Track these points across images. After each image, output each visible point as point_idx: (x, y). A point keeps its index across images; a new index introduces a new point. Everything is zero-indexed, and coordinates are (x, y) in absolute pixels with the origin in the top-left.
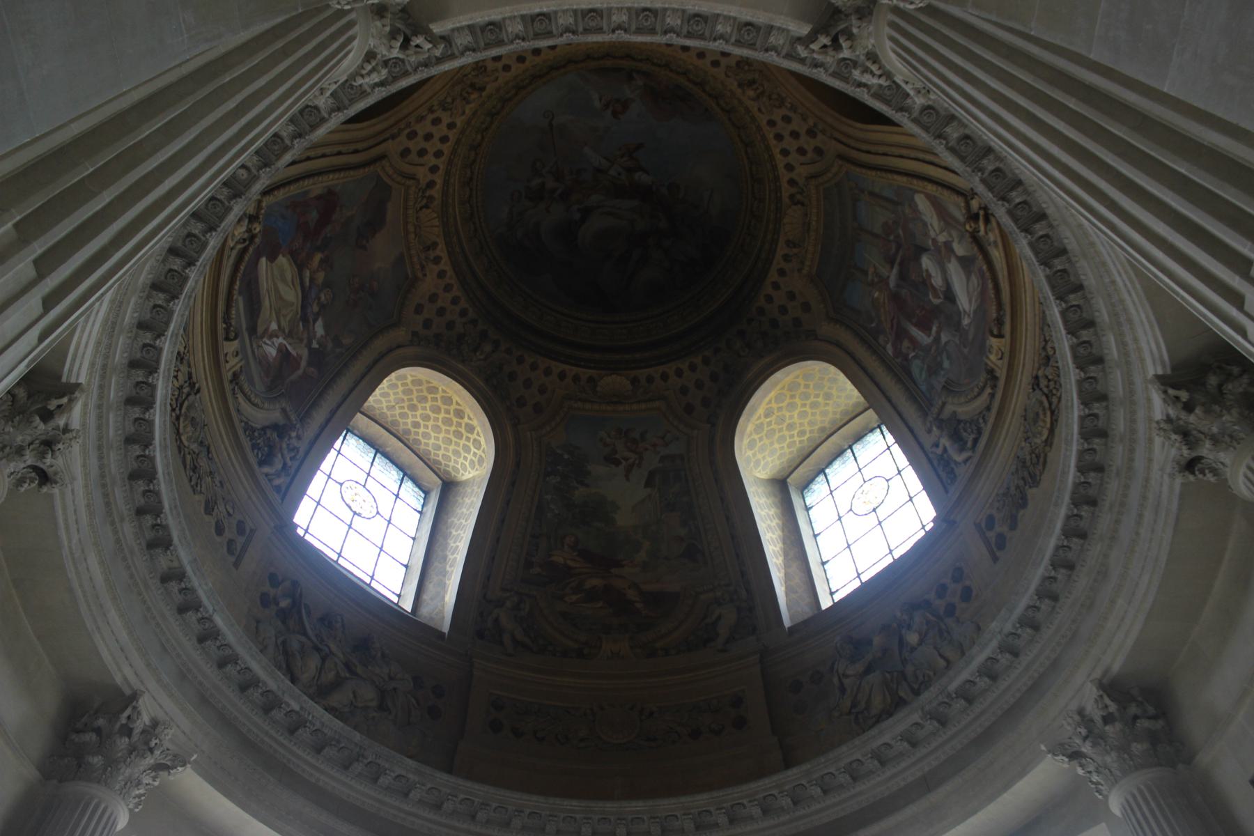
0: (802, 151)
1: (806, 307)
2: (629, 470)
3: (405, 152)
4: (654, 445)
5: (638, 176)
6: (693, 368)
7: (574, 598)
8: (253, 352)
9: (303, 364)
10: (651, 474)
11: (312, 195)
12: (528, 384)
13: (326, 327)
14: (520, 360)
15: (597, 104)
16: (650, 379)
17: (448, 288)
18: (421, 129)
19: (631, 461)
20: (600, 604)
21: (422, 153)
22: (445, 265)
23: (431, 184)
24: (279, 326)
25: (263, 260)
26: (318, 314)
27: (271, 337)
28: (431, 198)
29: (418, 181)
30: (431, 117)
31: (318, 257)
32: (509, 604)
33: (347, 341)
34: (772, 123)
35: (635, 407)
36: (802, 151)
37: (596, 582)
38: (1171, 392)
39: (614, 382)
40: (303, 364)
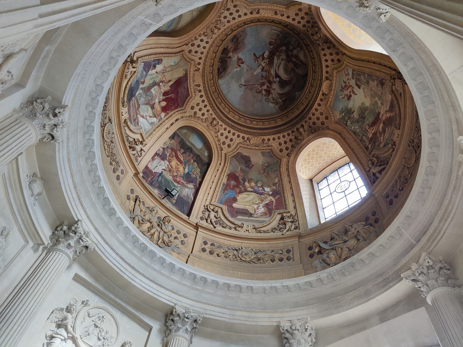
2: (354, 93)
3: (229, 146)
4: (348, 79)
5: (265, 56)
6: (325, 55)
7: (382, 138)
8: (257, 217)
9: (273, 200)
10: (357, 85)
11: (226, 182)
13: (269, 186)
14: (310, 119)
15: (238, 69)
17: (279, 138)
18: (223, 139)
19: (351, 91)
20: (387, 129)
22: (271, 137)
23: (243, 138)
24: (258, 204)
25: (235, 205)
26: (263, 188)
27: (258, 209)
28: (248, 138)
29: (240, 143)
30: (220, 136)
31: (247, 184)
32: (370, 166)
33: (276, 180)
35: (334, 82)
37: (381, 125)
40: (273, 200)
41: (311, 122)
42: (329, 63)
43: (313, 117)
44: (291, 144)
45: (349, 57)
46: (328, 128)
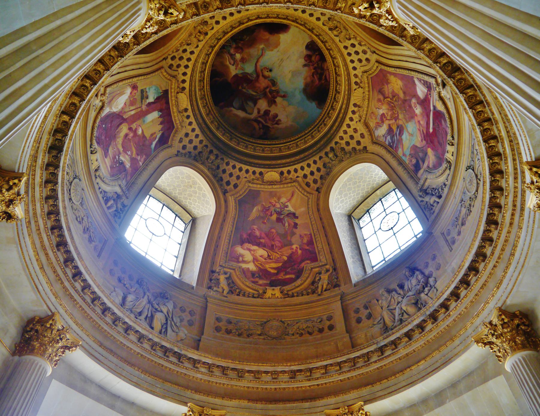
0: (360, 61)
1: (362, 136)
12: (231, 175)
14: (228, 164)
16: (289, 172)
17: (193, 130)
21: (179, 66)
34: (346, 48)
36: (360, 61)
38: (535, 169)
39: (272, 175)
41: (224, 166)
42: (301, 173)
43: (230, 167)
44: (192, 150)
45: (318, 199)
46: (225, 192)
